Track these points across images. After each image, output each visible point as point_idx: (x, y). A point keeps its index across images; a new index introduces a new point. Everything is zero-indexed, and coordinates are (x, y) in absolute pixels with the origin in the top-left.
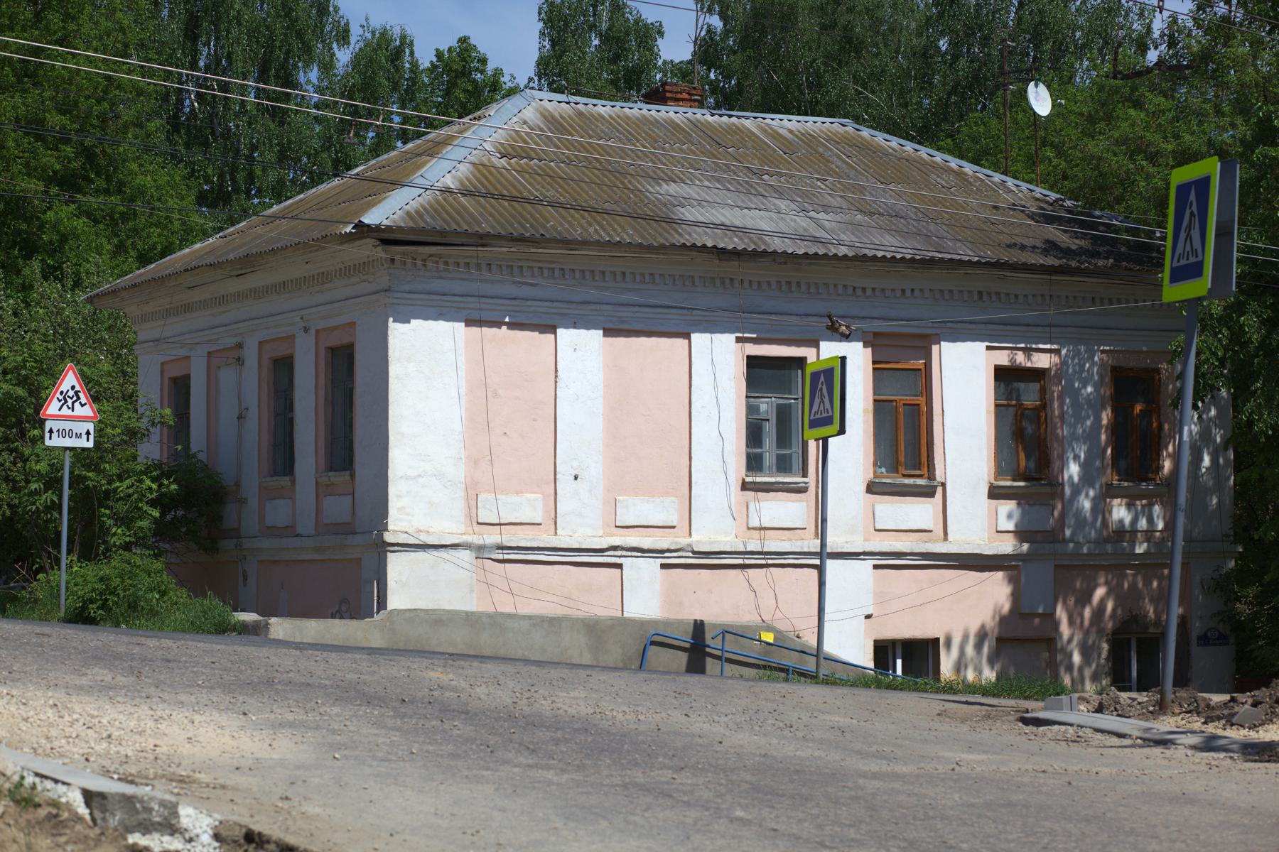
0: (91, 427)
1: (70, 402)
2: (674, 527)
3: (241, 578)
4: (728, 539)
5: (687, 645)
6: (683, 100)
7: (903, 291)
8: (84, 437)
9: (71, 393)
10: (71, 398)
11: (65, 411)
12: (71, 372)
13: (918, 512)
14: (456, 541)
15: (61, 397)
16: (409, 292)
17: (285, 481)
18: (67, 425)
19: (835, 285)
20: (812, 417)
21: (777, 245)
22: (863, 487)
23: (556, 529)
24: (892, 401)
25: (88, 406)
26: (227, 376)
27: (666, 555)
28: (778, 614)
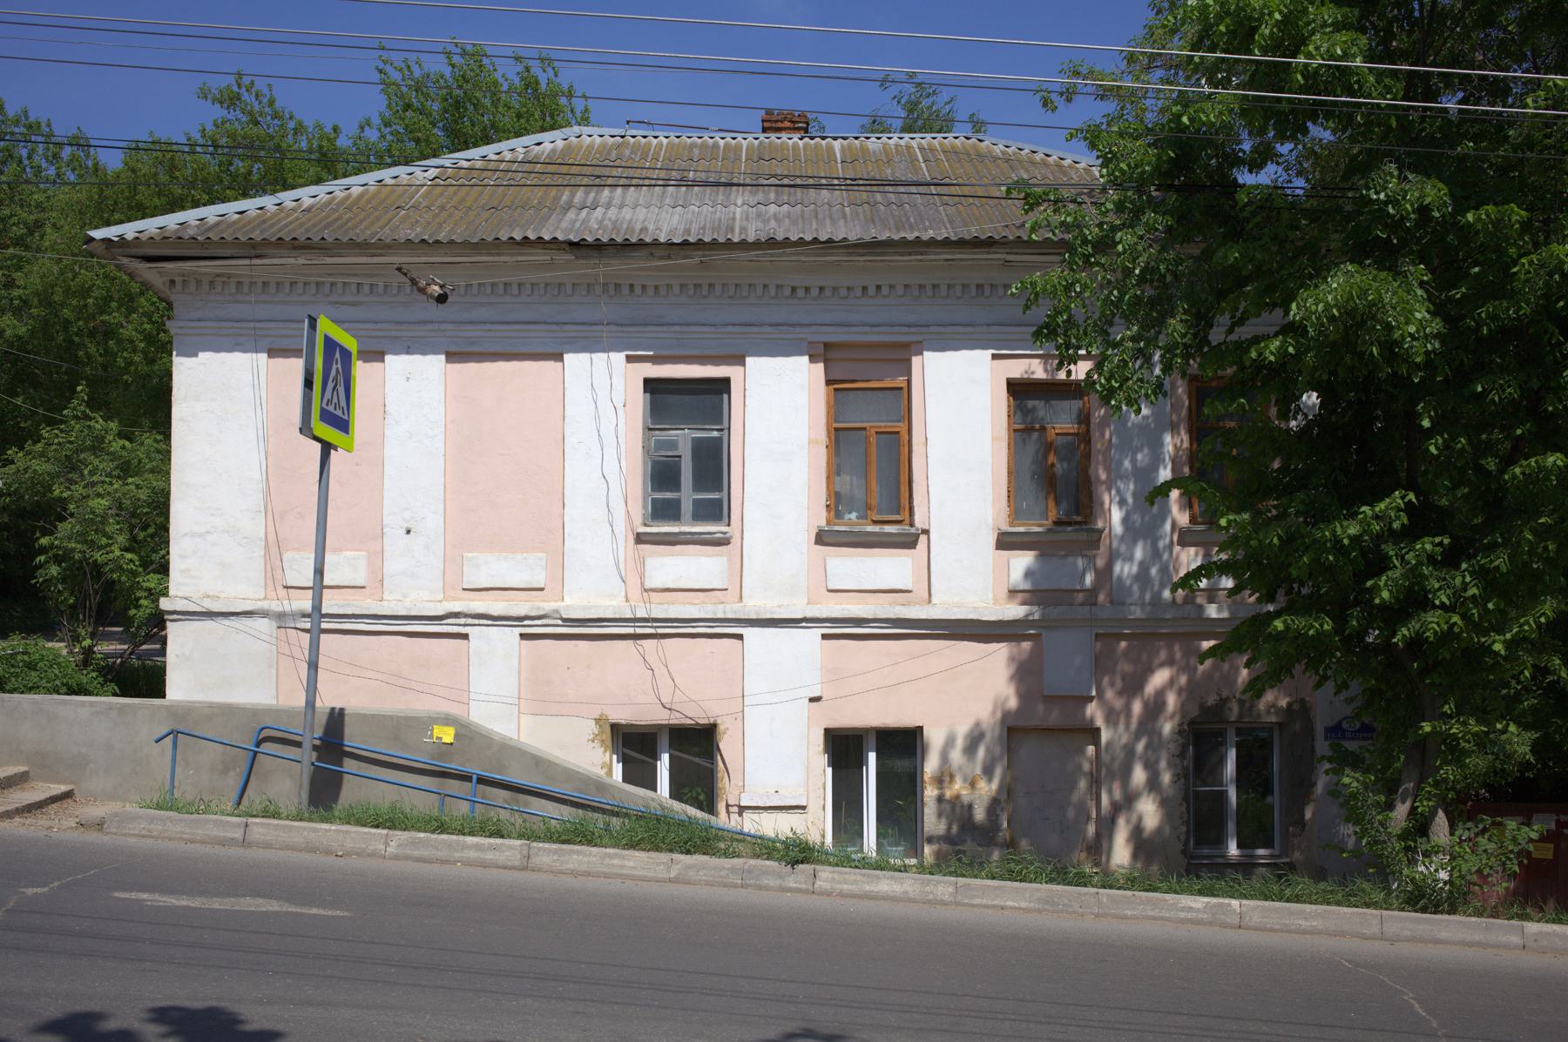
2: (542, 589)
4: (614, 603)
7: (865, 288)
14: (249, 608)
16: (199, 320)
27: (526, 623)
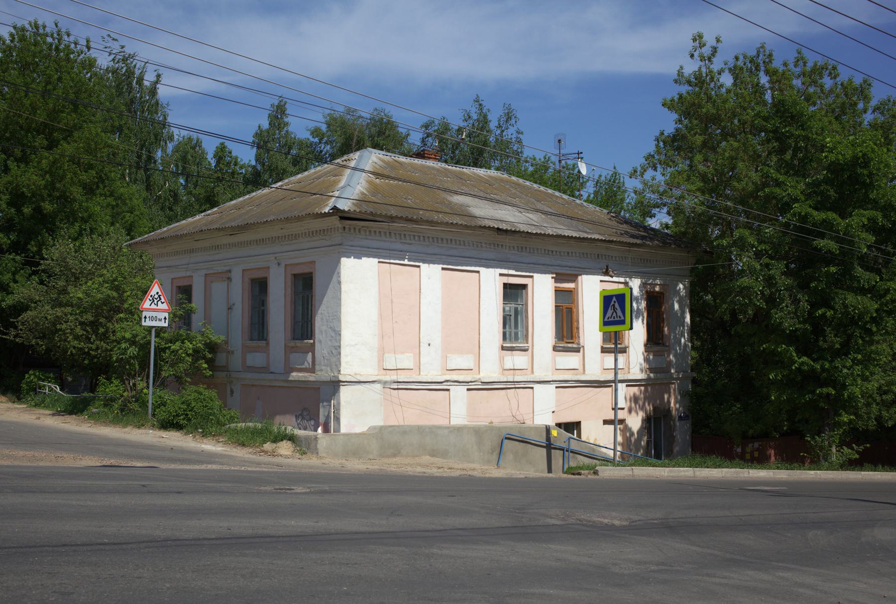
0: (166, 315)
1: (156, 301)
2: (472, 370)
3: (229, 392)
4: (495, 375)
5: (545, 445)
6: (432, 158)
7: (568, 253)
8: (163, 320)
9: (156, 296)
10: (156, 299)
11: (153, 306)
12: (156, 284)
13: (570, 360)
14: (374, 379)
15: (151, 299)
16: (352, 246)
17: (262, 343)
18: (154, 314)
19: (541, 249)
20: (606, 320)
21: (523, 228)
22: (551, 348)
23: (420, 371)
24: (559, 306)
25: (165, 303)
26: (218, 288)
27: (470, 384)
28: (518, 413)
